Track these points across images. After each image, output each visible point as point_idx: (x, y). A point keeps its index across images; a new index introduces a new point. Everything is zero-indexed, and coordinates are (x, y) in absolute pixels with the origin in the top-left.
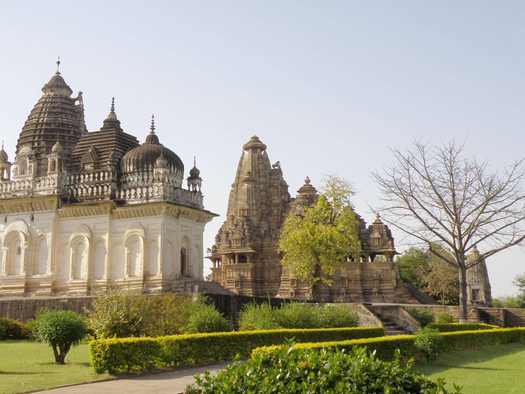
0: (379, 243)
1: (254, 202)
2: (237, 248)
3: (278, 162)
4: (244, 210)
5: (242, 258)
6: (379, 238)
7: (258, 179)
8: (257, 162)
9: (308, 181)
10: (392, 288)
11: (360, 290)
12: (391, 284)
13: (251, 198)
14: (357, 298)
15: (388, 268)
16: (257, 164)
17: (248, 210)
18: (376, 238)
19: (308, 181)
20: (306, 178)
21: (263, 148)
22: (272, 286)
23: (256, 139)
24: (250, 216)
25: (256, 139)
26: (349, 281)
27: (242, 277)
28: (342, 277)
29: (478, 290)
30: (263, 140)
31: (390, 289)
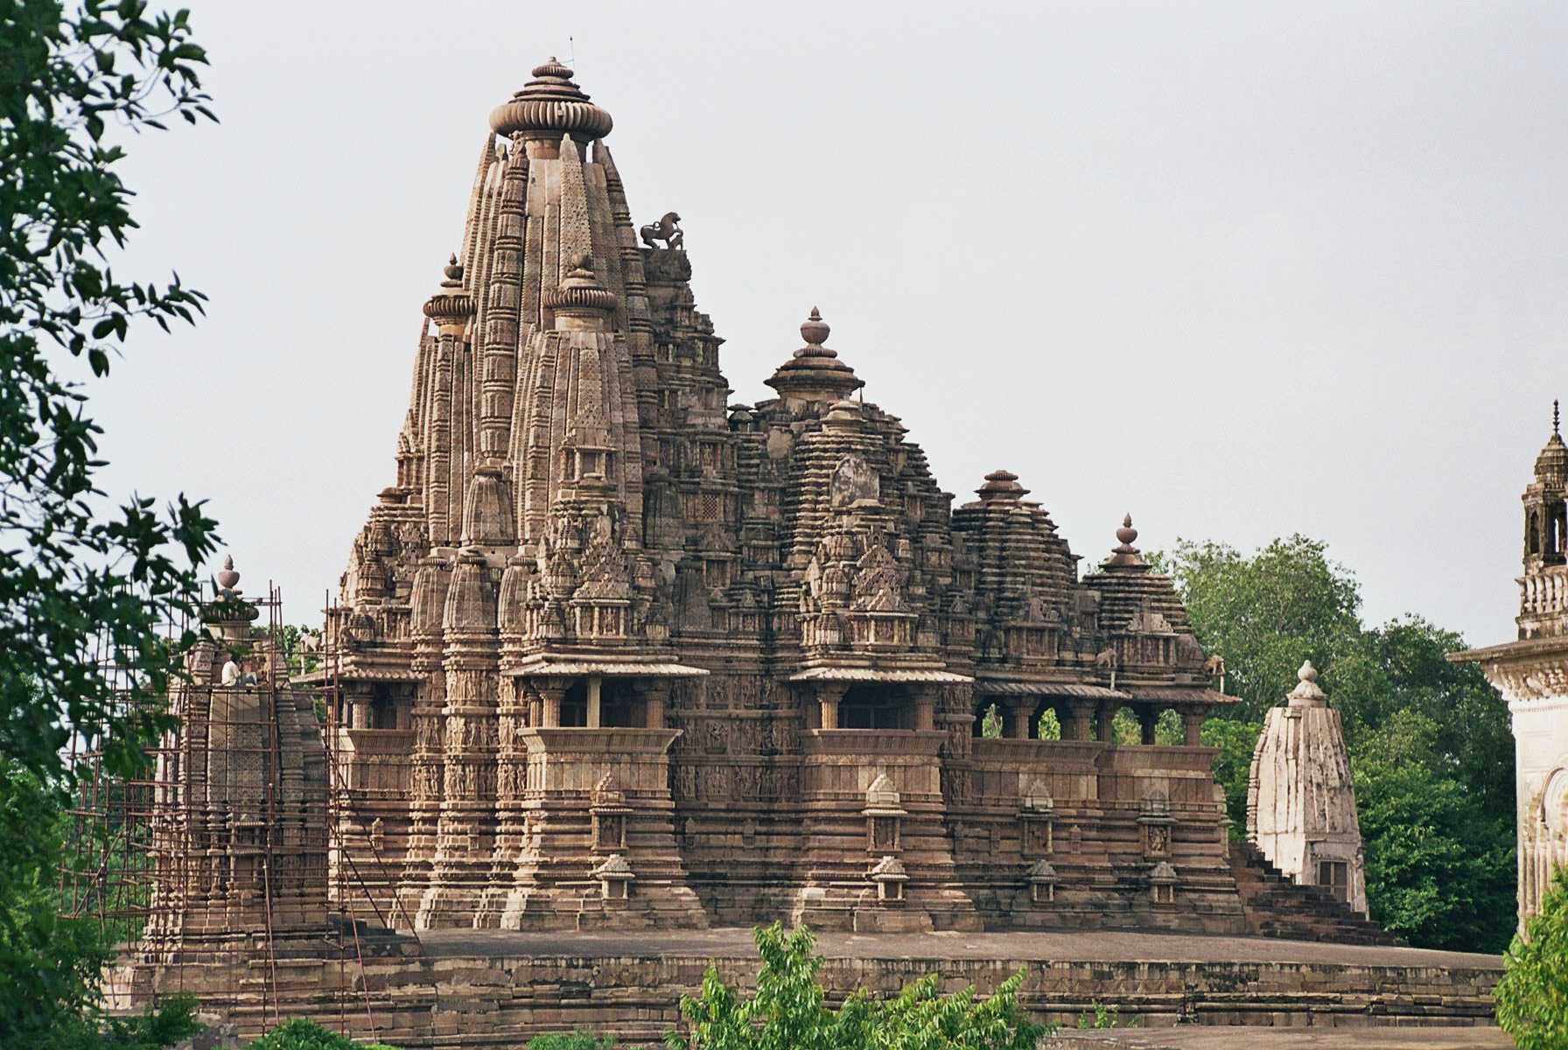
1: (634, 417)
2: (607, 647)
3: (674, 218)
4: (590, 456)
5: (624, 697)
6: (1167, 640)
9: (816, 333)
14: (1100, 906)
16: (610, 220)
17: (610, 454)
18: (1155, 638)
19: (816, 333)
20: (805, 319)
21: (592, 128)
22: (714, 840)
23: (557, 81)
25: (557, 81)
27: (632, 794)
28: (1032, 810)
29: (1341, 866)
30: (601, 91)
31: (1218, 871)
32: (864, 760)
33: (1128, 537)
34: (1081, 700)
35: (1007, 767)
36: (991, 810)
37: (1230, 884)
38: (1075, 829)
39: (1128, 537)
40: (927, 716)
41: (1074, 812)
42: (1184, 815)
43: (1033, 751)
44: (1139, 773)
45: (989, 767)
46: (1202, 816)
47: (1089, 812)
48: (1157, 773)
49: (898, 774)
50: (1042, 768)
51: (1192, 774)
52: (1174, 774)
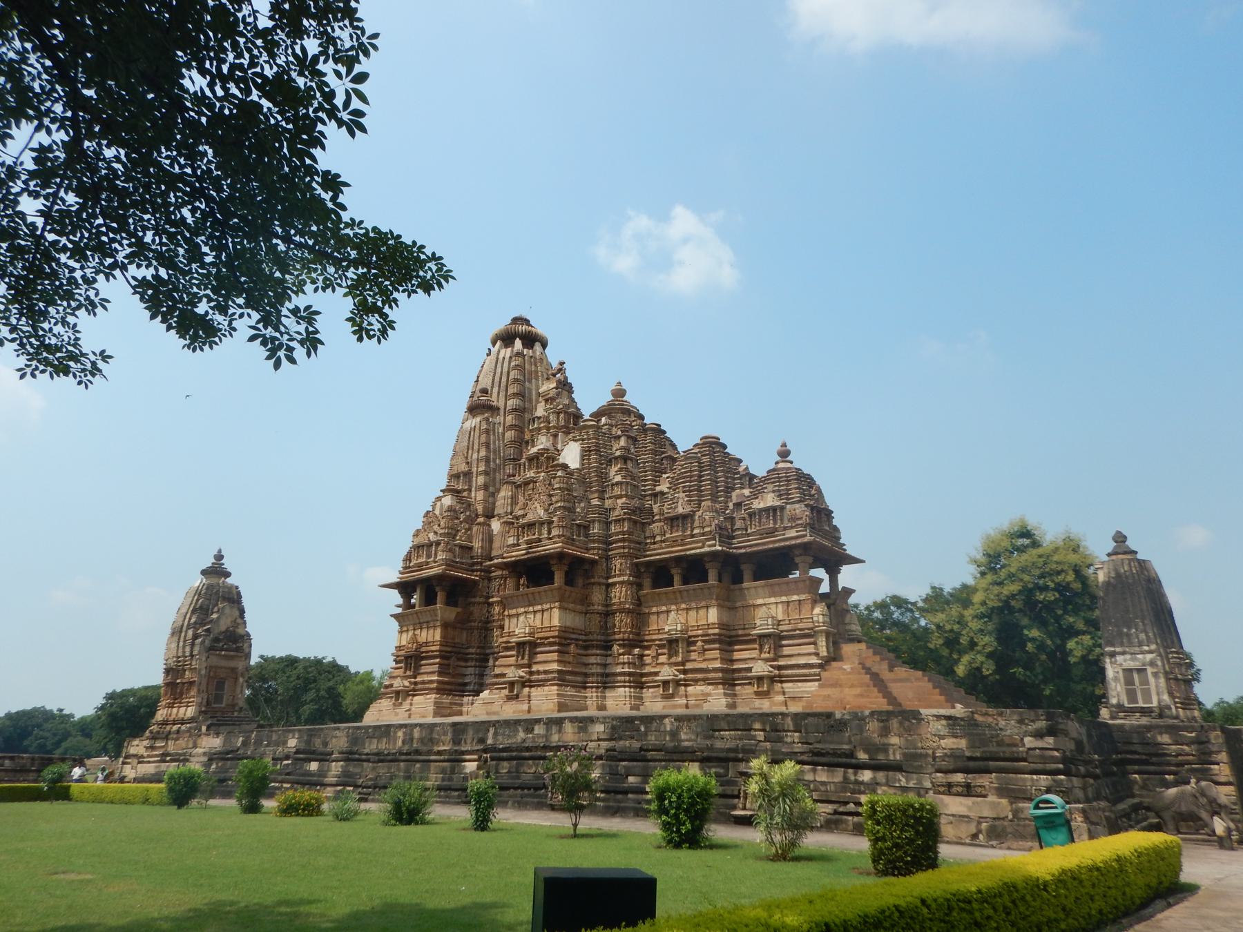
0: (775, 523)
7: (501, 404)
8: (506, 365)
9: (619, 393)
10: (814, 660)
11: (715, 670)
12: (811, 649)
13: (476, 447)
15: (803, 597)
16: (505, 369)
19: (619, 393)
24: (470, 490)
26: (690, 642)
32: (522, 610)
33: (784, 454)
34: (702, 555)
35: (664, 608)
36: (654, 637)
37: (815, 675)
38: (699, 644)
39: (784, 454)
40: (559, 578)
41: (700, 632)
42: (789, 627)
43: (678, 595)
44: (760, 601)
45: (654, 610)
46: (801, 626)
47: (711, 631)
48: (773, 600)
49: (539, 616)
50: (683, 606)
51: (795, 597)
52: (784, 599)
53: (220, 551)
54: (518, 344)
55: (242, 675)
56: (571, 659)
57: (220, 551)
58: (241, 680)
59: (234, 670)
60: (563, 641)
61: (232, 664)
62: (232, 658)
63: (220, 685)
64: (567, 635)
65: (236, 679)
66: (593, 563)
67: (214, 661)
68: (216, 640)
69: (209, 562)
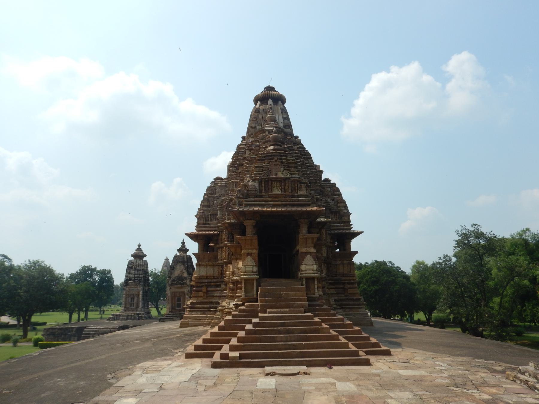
53: (183, 240)
54: (270, 102)
55: (187, 294)
56: (202, 295)
57: (183, 240)
58: (187, 296)
59: (183, 292)
60: (199, 285)
61: (182, 290)
62: (182, 288)
63: (179, 300)
64: (201, 281)
65: (185, 296)
66: (218, 235)
67: (173, 290)
68: (174, 281)
69: (179, 246)
